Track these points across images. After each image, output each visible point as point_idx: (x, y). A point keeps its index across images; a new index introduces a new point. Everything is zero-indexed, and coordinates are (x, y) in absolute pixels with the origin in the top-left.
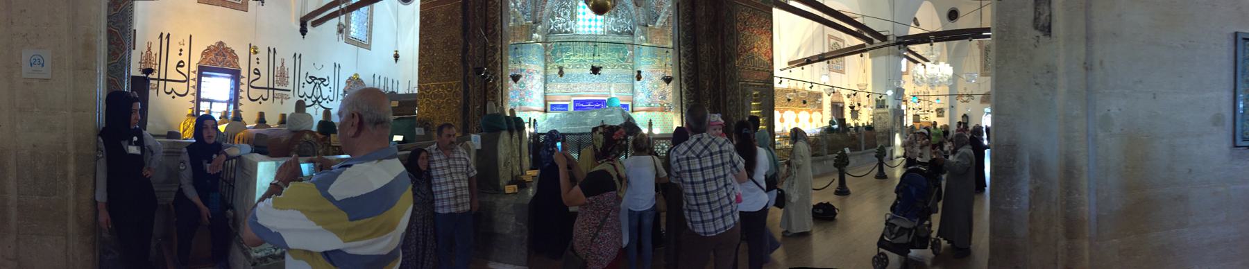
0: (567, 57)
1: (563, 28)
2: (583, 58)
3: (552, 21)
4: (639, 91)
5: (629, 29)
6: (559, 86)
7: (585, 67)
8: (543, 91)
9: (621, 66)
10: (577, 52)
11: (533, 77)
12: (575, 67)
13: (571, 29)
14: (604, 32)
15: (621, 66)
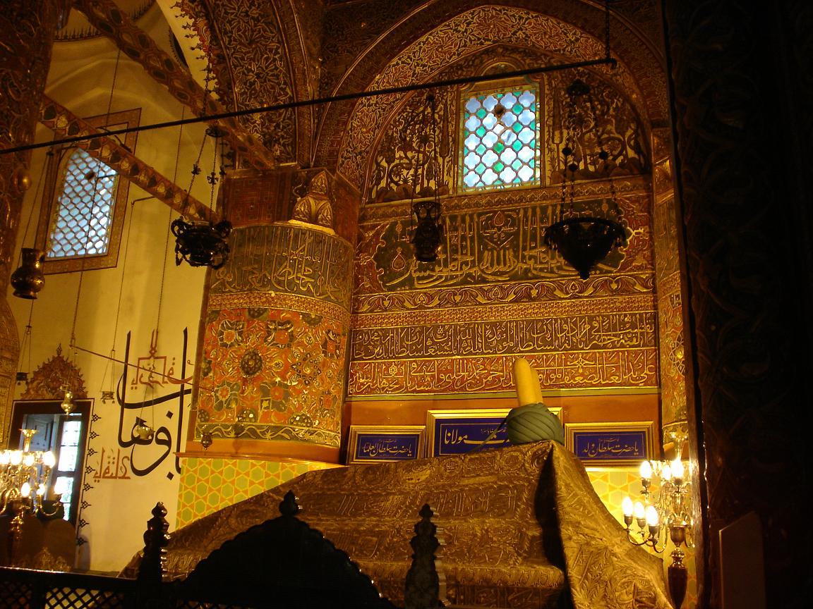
1: (415, 183)
3: (384, 164)
5: (631, 153)
6: (393, 370)
7: (480, 299)
9: (605, 284)
10: (455, 251)
11: (292, 337)
13: (440, 184)
14: (542, 177)
15: (605, 284)
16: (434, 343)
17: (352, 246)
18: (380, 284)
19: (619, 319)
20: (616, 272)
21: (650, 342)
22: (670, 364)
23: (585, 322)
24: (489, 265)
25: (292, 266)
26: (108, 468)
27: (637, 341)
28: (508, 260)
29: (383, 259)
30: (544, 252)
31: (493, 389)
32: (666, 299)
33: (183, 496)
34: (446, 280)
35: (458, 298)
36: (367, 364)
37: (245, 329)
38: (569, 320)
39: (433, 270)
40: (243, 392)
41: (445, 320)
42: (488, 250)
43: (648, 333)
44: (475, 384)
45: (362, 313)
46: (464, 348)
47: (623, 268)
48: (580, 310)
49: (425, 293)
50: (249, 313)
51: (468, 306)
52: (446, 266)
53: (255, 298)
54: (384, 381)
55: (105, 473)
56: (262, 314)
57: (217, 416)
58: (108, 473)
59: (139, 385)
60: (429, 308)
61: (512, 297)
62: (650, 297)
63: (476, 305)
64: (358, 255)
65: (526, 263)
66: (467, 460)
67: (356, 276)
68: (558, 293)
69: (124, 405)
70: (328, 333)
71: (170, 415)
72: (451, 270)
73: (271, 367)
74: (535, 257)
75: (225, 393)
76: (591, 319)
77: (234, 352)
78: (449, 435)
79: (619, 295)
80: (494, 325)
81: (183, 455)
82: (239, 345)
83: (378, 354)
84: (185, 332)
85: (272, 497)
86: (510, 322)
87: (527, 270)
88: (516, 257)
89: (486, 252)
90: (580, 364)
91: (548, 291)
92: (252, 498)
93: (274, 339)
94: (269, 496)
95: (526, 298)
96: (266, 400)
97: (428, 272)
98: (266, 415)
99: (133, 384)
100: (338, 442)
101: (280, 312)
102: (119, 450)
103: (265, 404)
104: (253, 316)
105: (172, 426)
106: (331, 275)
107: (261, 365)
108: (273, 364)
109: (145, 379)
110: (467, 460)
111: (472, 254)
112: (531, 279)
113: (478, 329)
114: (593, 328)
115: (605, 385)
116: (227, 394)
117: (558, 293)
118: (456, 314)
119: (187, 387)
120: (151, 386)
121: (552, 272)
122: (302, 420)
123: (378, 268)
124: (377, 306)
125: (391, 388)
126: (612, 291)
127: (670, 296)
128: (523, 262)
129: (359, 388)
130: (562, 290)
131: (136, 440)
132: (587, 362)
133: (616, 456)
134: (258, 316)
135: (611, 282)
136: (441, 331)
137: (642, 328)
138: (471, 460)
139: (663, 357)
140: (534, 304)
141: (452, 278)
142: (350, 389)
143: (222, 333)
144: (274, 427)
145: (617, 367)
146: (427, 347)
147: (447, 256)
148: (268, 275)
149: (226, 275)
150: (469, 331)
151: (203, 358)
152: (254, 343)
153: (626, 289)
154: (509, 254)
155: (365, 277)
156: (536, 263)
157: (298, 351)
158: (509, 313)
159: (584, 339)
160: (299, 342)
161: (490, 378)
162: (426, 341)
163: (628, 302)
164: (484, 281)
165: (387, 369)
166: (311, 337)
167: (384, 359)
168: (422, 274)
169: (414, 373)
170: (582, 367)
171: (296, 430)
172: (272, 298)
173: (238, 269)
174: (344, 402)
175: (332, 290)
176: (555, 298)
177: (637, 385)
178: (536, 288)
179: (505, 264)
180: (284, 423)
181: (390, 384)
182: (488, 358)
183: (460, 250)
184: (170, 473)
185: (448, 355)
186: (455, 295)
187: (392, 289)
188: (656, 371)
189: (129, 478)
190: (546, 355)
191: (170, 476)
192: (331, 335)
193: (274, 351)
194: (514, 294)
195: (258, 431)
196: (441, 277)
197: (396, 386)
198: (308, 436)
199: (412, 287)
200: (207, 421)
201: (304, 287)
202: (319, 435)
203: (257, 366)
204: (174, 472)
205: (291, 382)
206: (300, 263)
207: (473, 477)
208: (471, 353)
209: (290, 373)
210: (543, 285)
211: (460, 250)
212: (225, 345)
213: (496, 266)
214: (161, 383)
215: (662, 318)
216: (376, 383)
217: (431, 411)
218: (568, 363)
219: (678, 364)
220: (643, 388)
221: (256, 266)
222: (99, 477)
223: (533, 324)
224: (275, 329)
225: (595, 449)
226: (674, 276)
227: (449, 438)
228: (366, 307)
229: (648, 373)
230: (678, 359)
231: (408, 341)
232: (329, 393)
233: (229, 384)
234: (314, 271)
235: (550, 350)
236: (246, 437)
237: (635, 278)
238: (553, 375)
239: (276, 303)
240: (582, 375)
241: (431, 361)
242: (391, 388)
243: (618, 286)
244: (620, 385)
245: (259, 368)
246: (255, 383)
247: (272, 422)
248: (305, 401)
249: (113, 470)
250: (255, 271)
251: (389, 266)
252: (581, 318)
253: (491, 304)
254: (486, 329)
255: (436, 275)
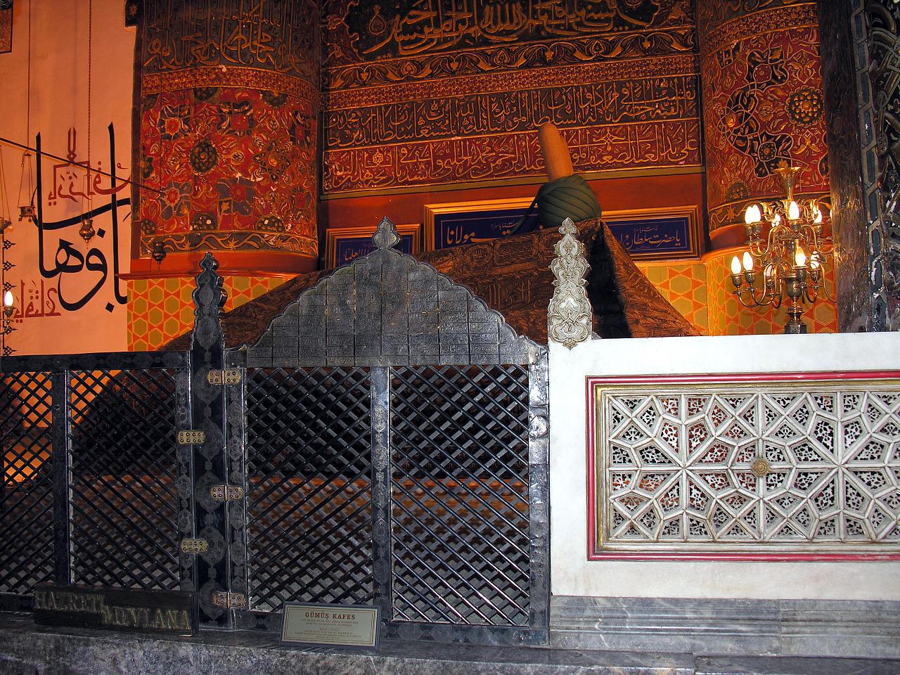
0: (407, 30)
2: (475, 31)
4: (722, 146)
6: (378, 158)
7: (483, 65)
8: (307, 184)
9: (636, 43)
10: (449, 8)
11: (252, 120)
12: (440, 69)
15: (636, 43)
16: (428, 123)
17: (316, 5)
18: (355, 53)
19: (654, 85)
20: (648, 28)
21: (691, 111)
22: (719, 135)
23: (612, 89)
24: (491, 23)
25: (245, 32)
26: (31, 304)
27: (675, 111)
28: (514, 16)
29: (356, 21)
30: (559, 5)
31: (504, 175)
32: (713, 55)
33: (133, 326)
34: (438, 44)
35: (454, 66)
36: (343, 153)
37: (192, 115)
38: (593, 88)
39: (422, 32)
40: (195, 194)
41: (439, 93)
42: (490, 5)
43: (688, 101)
44: (482, 169)
45: (335, 89)
46: (466, 127)
47: (657, 23)
48: (606, 75)
49: (413, 61)
50: (196, 94)
51: (468, 74)
52: (437, 26)
53: (201, 75)
54: (368, 172)
55: (28, 310)
56: (213, 94)
57: (165, 226)
58: (32, 310)
59: (58, 198)
60: (419, 79)
61: (522, 62)
62: (691, 58)
63: (478, 73)
64: (324, 17)
65: (537, 19)
66: (497, 246)
67: (324, 44)
68: (578, 55)
69: (42, 226)
70: (295, 115)
71: (101, 233)
72: (444, 31)
73: (229, 160)
74: (548, 11)
75: (173, 196)
76: (620, 85)
77: (180, 144)
78: (452, 233)
79: (652, 55)
80: (501, 96)
81: (125, 277)
82: (186, 135)
83: (358, 140)
84: (111, 128)
85: (259, 307)
86: (521, 92)
87: (539, 29)
88: (525, 11)
89: (487, 7)
90: (608, 141)
91: (566, 52)
92: (236, 309)
93: (229, 126)
94: (257, 306)
95: (540, 62)
96: (226, 202)
97: (415, 35)
98: (227, 222)
99: (50, 198)
100: (316, 250)
101: (234, 90)
102: (42, 282)
103: (225, 207)
104: (201, 98)
105: (105, 245)
106: (294, 42)
107: (216, 159)
108: (231, 156)
109: (65, 191)
110: (497, 246)
111: (470, 10)
112: (544, 38)
113: (481, 102)
114: (622, 96)
115: (638, 165)
116: (176, 198)
117: (578, 55)
118: (453, 85)
119: (120, 196)
120: (74, 199)
121: (571, 29)
122: (271, 224)
123: (351, 33)
124: (354, 79)
125: (376, 180)
126: (645, 51)
127: (718, 52)
128: (534, 19)
129: (337, 183)
130: (583, 52)
131: (62, 268)
132: (616, 138)
133: (654, 248)
134: (207, 98)
135: (644, 41)
136: (435, 107)
137: (681, 95)
138: (502, 246)
139: (709, 128)
140: (550, 70)
141: (446, 40)
142: (325, 184)
143: (162, 122)
144: (238, 234)
145: (653, 143)
146: (419, 129)
147: (438, 13)
148: (215, 45)
149: (162, 48)
150: (471, 107)
151: (141, 156)
152: (203, 133)
153: (660, 48)
154: (517, 8)
155: (335, 45)
156: (550, 18)
157: (259, 139)
158: (520, 81)
159: (611, 110)
160: (260, 127)
161: (499, 162)
162: (417, 121)
163: (664, 64)
164: (487, 43)
165: (370, 157)
166: (275, 121)
167: (365, 145)
168: (407, 38)
169: (404, 160)
170: (611, 144)
171: (266, 236)
172: (224, 74)
173: (176, 40)
174: (319, 201)
175: (297, 60)
176: (574, 61)
177: (677, 163)
178: (552, 50)
179: (511, 22)
180: (251, 228)
181: (375, 176)
182: (495, 138)
183: (454, 5)
184: (109, 304)
185: (446, 136)
186: (450, 61)
187: (371, 57)
188: (699, 147)
189: (59, 314)
190: (566, 131)
191: (110, 307)
192: (299, 118)
193: (231, 140)
194: (525, 57)
195: (219, 240)
196: (432, 40)
197: (382, 178)
198: (280, 244)
199: (395, 53)
200: (153, 232)
201: (262, 58)
202: (293, 241)
203: (211, 160)
204: (114, 302)
205: (255, 178)
206: (255, 28)
207: (507, 265)
208: (474, 133)
209: (252, 167)
210: (560, 46)
211: (454, 5)
212: (169, 137)
213: (500, 24)
214: (86, 194)
215: (708, 80)
216: (358, 175)
217: (429, 206)
218: (594, 140)
219: (729, 133)
220: (683, 167)
221: (200, 34)
222: (22, 316)
223: (550, 93)
224: (230, 113)
225: (630, 240)
226: (722, 28)
227: (452, 237)
228: (339, 82)
229: (690, 148)
230: (728, 127)
231: (394, 121)
232: (302, 189)
233: (177, 185)
234: (273, 37)
235: (572, 125)
236: (204, 249)
237: (672, 35)
238: (576, 154)
239: (228, 80)
240: (611, 153)
241: (424, 145)
242: (376, 180)
243: (651, 45)
244: (657, 163)
245: (214, 163)
246: (210, 182)
247: (235, 228)
248: (273, 201)
249: (37, 306)
250: (198, 41)
251: (365, 29)
252: (608, 85)
253: (497, 71)
254: (491, 102)
255: (425, 38)
